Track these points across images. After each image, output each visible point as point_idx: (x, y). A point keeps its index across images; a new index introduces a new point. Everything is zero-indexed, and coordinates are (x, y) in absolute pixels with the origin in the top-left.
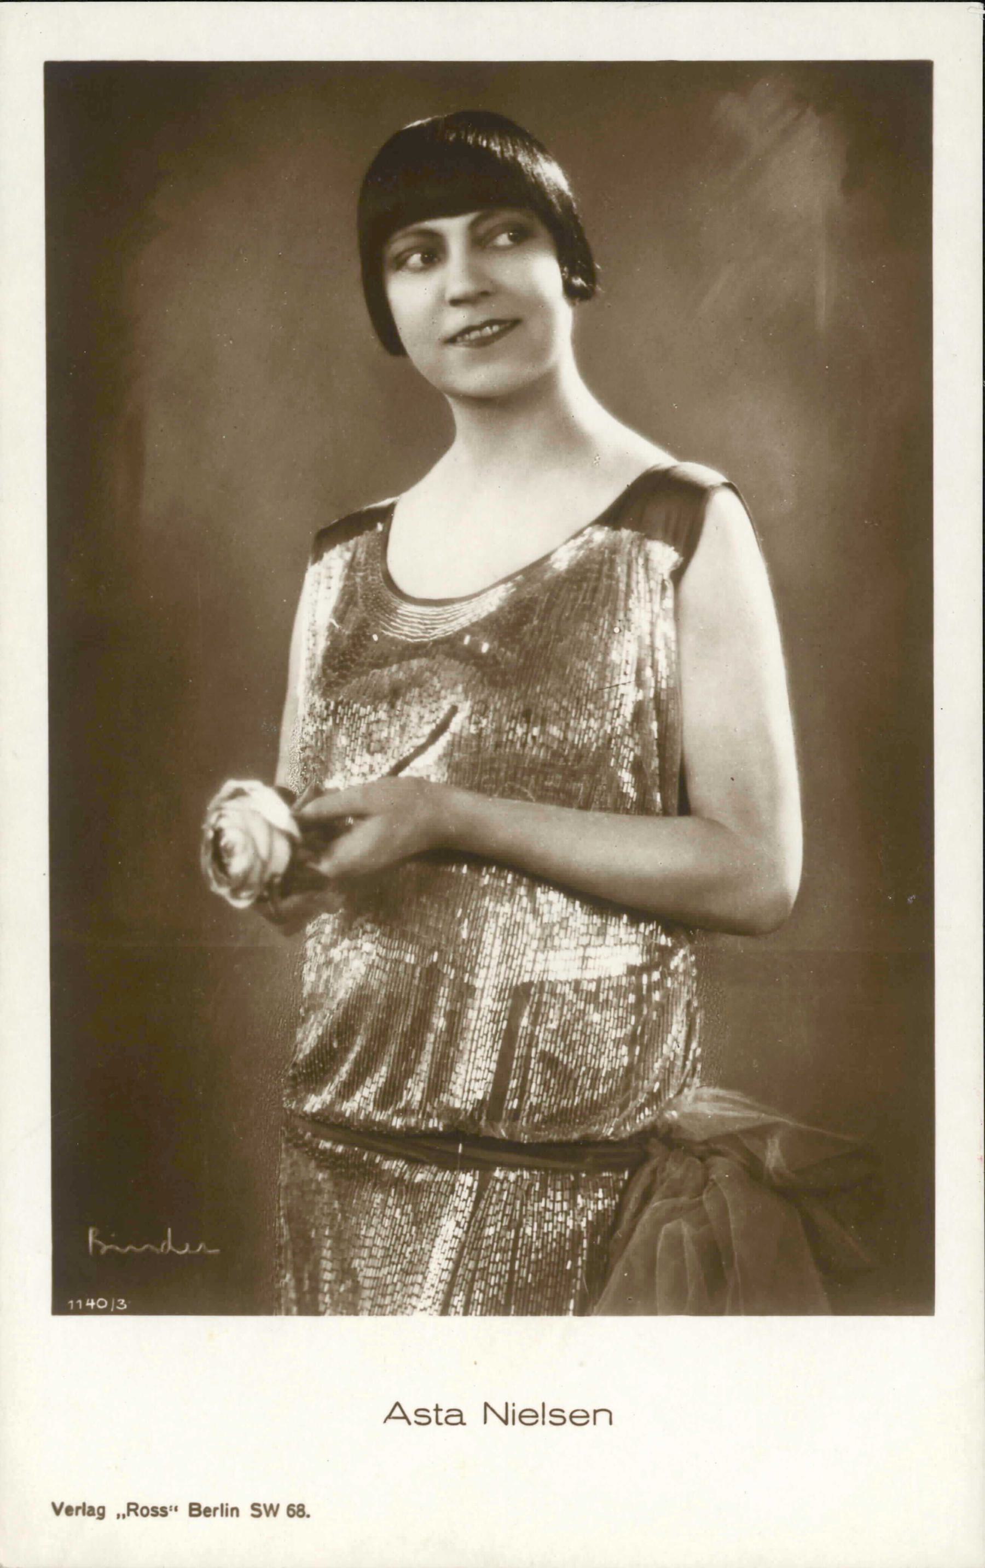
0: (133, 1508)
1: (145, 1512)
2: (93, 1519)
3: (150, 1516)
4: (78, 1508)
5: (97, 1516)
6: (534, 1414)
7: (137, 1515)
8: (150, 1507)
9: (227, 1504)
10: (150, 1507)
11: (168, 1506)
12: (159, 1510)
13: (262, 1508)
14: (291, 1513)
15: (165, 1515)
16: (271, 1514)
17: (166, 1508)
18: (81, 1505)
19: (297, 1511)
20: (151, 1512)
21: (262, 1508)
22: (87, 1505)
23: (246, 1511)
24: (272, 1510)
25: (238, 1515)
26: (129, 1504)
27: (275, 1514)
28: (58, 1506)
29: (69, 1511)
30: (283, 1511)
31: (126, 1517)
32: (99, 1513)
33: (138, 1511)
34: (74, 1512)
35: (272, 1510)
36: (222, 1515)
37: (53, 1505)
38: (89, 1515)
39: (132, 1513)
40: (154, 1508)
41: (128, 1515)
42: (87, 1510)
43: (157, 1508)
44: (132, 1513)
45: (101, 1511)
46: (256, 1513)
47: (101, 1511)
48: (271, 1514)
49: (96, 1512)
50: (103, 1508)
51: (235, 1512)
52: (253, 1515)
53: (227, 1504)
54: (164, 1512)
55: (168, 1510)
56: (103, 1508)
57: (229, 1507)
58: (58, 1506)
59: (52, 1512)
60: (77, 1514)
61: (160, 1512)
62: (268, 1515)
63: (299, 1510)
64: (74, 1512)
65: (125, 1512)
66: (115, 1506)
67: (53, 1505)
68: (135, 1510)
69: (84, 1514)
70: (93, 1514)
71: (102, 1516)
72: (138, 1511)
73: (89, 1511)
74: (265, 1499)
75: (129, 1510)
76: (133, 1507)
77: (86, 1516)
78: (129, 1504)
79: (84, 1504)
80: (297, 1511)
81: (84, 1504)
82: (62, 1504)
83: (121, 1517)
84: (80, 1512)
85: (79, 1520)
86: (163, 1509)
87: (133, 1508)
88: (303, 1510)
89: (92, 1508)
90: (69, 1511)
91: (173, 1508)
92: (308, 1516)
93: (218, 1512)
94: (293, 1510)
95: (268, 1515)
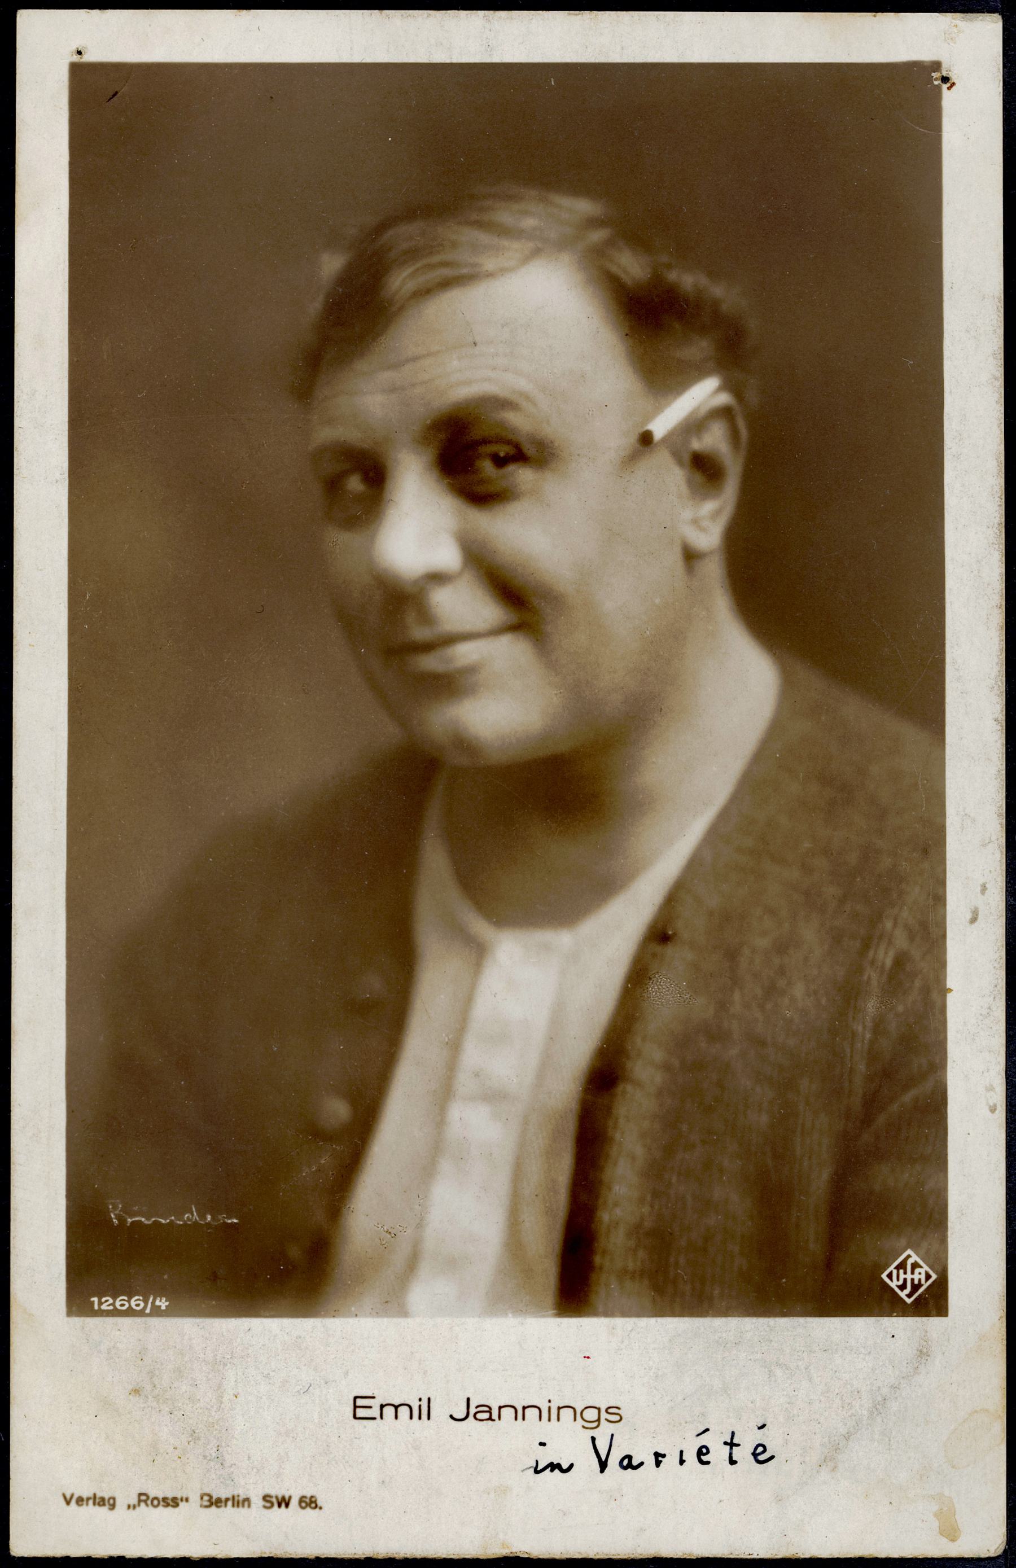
0: (143, 1498)
1: (156, 1502)
2: (104, 1510)
5: (107, 1506)
7: (147, 1505)
9: (238, 1496)
11: (179, 1497)
12: (170, 1501)
13: (274, 1500)
14: (303, 1505)
15: (176, 1505)
16: (283, 1505)
19: (309, 1503)
20: (162, 1503)
21: (274, 1500)
22: (98, 1496)
23: (257, 1502)
24: (284, 1502)
25: (249, 1506)
26: (140, 1495)
27: (287, 1505)
28: (68, 1497)
29: (80, 1501)
30: (294, 1502)
32: (110, 1505)
33: (149, 1502)
35: (284, 1502)
36: (233, 1506)
38: (99, 1505)
39: (143, 1504)
40: (165, 1499)
41: (139, 1505)
42: (97, 1500)
44: (143, 1504)
45: (111, 1501)
46: (268, 1505)
47: (111, 1501)
48: (283, 1505)
49: (107, 1503)
50: (114, 1499)
51: (246, 1504)
52: (265, 1507)
53: (238, 1496)
54: (173, 1502)
57: (241, 1499)
58: (68, 1497)
59: (64, 1503)
60: (87, 1504)
61: (171, 1503)
62: (280, 1506)
63: (311, 1502)
66: (125, 1496)
68: (145, 1501)
69: (94, 1504)
70: (104, 1505)
71: (113, 1507)
72: (149, 1502)
73: (100, 1501)
74: (277, 1491)
75: (140, 1501)
76: (143, 1498)
77: (97, 1507)
79: (95, 1495)
80: (309, 1503)
81: (95, 1495)
82: (72, 1496)
85: (90, 1510)
86: (174, 1499)
87: (143, 1498)
88: (315, 1502)
89: (103, 1499)
90: (80, 1501)
91: (184, 1499)
92: (321, 1508)
93: (230, 1503)
94: (306, 1502)
95: (280, 1506)
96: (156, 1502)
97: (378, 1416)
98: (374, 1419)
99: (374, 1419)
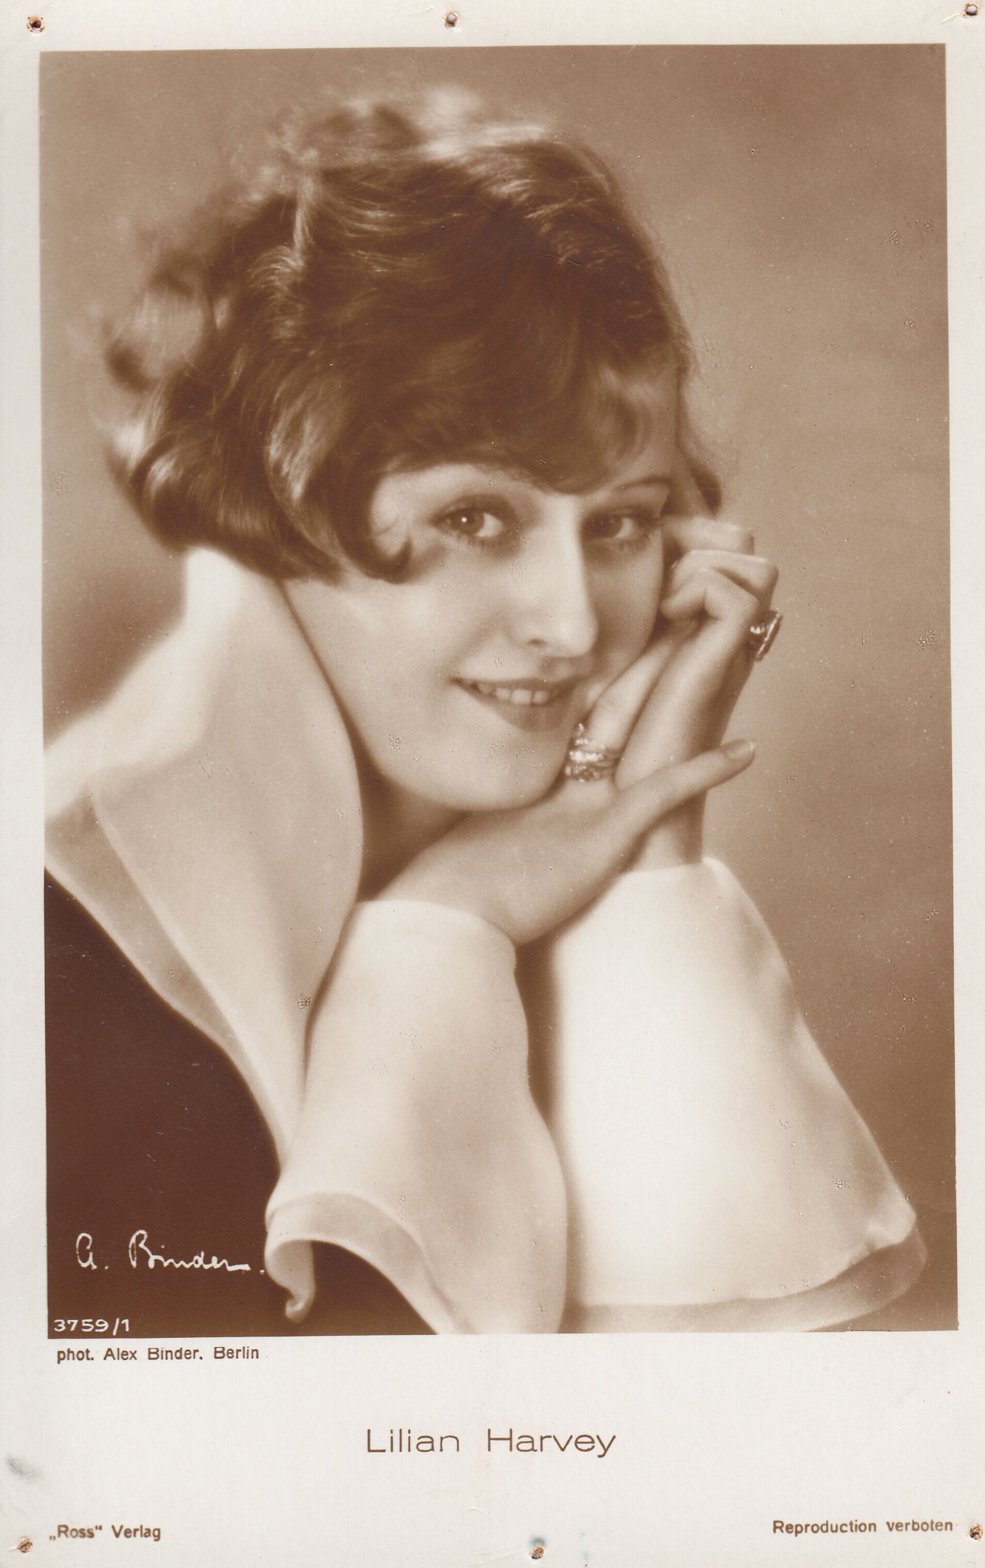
0: (63, 1530)
4: (136, 1530)
6: (590, 1440)
18: (139, 1527)
26: (59, 1527)
29: (128, 1533)
31: (57, 1538)
32: (154, 1535)
34: (132, 1534)
37: (113, 1527)
39: (62, 1535)
40: (82, 1531)
42: (144, 1532)
43: (84, 1530)
45: (156, 1533)
50: (159, 1530)
56: (159, 1530)
60: (135, 1536)
67: (113, 1527)
78: (59, 1527)
79: (141, 1526)
81: (141, 1526)
84: (138, 1533)
87: (63, 1530)
89: (148, 1530)
90: (128, 1533)
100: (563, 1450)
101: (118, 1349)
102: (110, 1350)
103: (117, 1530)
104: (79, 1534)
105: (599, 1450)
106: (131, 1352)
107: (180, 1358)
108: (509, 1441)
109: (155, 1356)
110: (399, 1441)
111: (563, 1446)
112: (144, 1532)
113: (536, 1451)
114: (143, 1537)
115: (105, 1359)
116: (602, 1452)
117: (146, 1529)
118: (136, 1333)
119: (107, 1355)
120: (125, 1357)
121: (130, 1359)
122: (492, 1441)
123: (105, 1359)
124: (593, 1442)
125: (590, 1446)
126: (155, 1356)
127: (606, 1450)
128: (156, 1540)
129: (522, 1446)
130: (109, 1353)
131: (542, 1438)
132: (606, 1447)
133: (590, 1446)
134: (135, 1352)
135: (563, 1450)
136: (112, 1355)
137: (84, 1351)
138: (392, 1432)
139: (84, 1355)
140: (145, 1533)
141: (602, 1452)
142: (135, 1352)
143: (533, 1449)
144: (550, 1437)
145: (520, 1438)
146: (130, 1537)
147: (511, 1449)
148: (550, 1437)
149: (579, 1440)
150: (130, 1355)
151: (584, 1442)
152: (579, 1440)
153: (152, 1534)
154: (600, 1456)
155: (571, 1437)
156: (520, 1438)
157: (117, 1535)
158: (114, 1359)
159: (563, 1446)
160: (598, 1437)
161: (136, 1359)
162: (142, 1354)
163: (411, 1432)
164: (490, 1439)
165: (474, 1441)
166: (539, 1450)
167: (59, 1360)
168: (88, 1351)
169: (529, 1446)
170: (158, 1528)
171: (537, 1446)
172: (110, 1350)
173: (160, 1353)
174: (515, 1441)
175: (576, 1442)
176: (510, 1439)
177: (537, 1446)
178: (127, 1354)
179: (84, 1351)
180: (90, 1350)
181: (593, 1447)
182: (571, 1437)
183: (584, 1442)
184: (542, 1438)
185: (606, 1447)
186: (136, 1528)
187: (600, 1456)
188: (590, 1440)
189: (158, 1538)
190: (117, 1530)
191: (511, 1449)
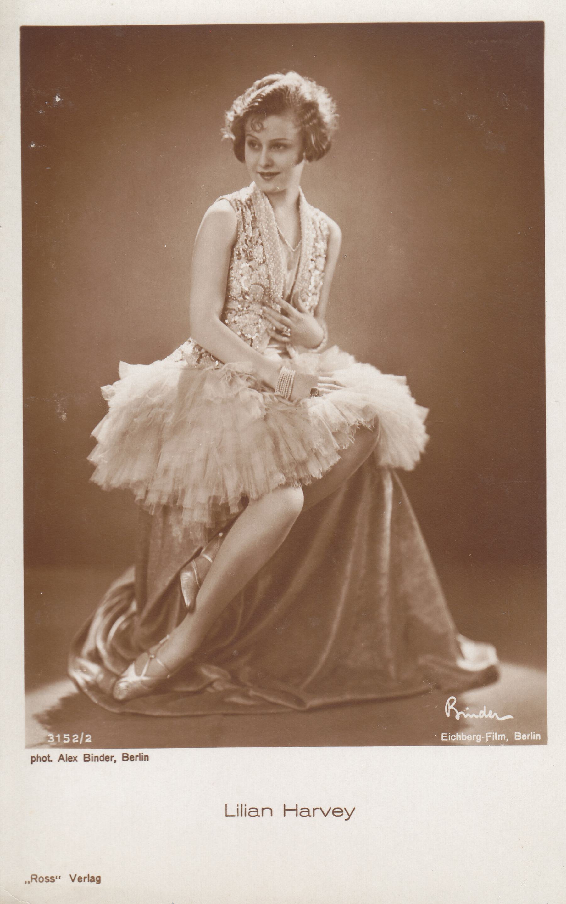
1: (41, 879)
2: (94, 883)
3: (44, 882)
5: (96, 882)
6: (340, 811)
7: (36, 881)
8: (44, 877)
10: (44, 877)
17: (54, 877)
22: (90, 876)
29: (80, 879)
32: (97, 880)
34: (83, 880)
41: (32, 881)
42: (90, 878)
44: (34, 881)
50: (99, 877)
55: (55, 879)
56: (99, 877)
64: (83, 880)
65: (30, 880)
68: (35, 879)
70: (94, 881)
72: (37, 879)
75: (32, 879)
76: (34, 877)
79: (88, 875)
81: (88, 875)
83: (27, 883)
84: (86, 879)
89: (93, 877)
90: (80, 879)
96: (41, 879)
97: (236, 814)
98: (235, 816)
99: (235, 816)
100: (325, 816)
101: (66, 755)
102: (61, 755)
103: (73, 878)
104: (45, 880)
105: (346, 816)
106: (74, 757)
107: (103, 761)
108: (295, 811)
109: (87, 759)
110: (242, 811)
111: (325, 813)
112: (90, 878)
113: (311, 816)
114: (90, 882)
115: (59, 761)
116: (347, 817)
117: (91, 877)
118: (94, 745)
119: (60, 759)
120: (70, 760)
121: (74, 761)
122: (286, 811)
123: (59, 761)
124: (342, 812)
125: (340, 814)
126: (87, 759)
127: (350, 816)
128: (97, 883)
129: (303, 814)
130: (61, 757)
131: (314, 809)
132: (350, 814)
133: (340, 814)
134: (77, 757)
135: (325, 816)
136: (63, 759)
137: (47, 756)
138: (238, 805)
139: (46, 759)
140: (91, 879)
141: (347, 817)
142: (77, 757)
143: (309, 816)
144: (318, 808)
145: (301, 809)
146: (81, 881)
147: (297, 816)
148: (318, 808)
149: (335, 811)
150: (73, 759)
151: (337, 812)
152: (335, 811)
153: (95, 880)
154: (346, 820)
155: (330, 808)
156: (301, 809)
157: (73, 881)
158: (64, 761)
159: (325, 814)
160: (345, 809)
161: (77, 761)
162: (80, 758)
163: (247, 805)
164: (285, 810)
165: (278, 811)
166: (312, 816)
167: (32, 762)
168: (49, 756)
169: (306, 814)
170: (99, 875)
171: (311, 814)
172: (61, 755)
173: (91, 758)
174: (299, 811)
175: (333, 812)
176: (296, 810)
177: (311, 814)
178: (72, 758)
179: (47, 756)
180: (50, 756)
181: (342, 815)
182: (330, 808)
183: (337, 812)
184: (314, 809)
185: (350, 814)
186: (85, 876)
187: (346, 820)
188: (340, 811)
189: (99, 882)
190: (73, 878)
191: (297, 816)
